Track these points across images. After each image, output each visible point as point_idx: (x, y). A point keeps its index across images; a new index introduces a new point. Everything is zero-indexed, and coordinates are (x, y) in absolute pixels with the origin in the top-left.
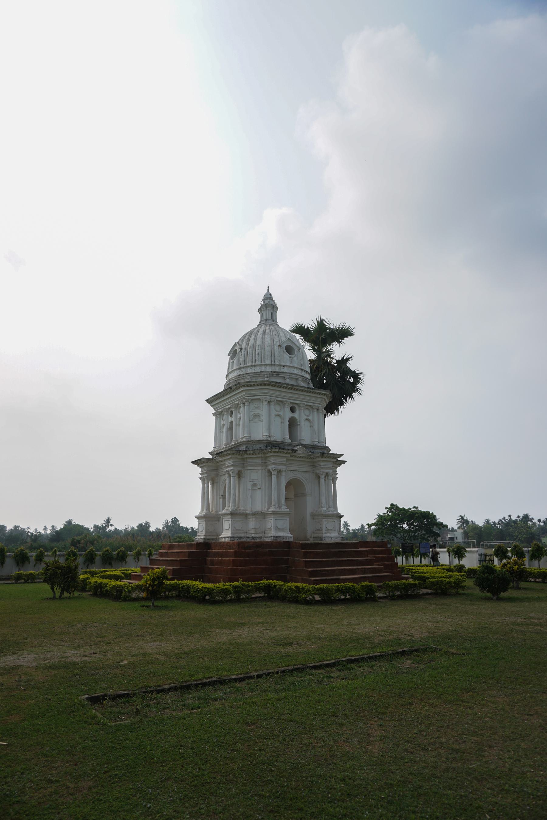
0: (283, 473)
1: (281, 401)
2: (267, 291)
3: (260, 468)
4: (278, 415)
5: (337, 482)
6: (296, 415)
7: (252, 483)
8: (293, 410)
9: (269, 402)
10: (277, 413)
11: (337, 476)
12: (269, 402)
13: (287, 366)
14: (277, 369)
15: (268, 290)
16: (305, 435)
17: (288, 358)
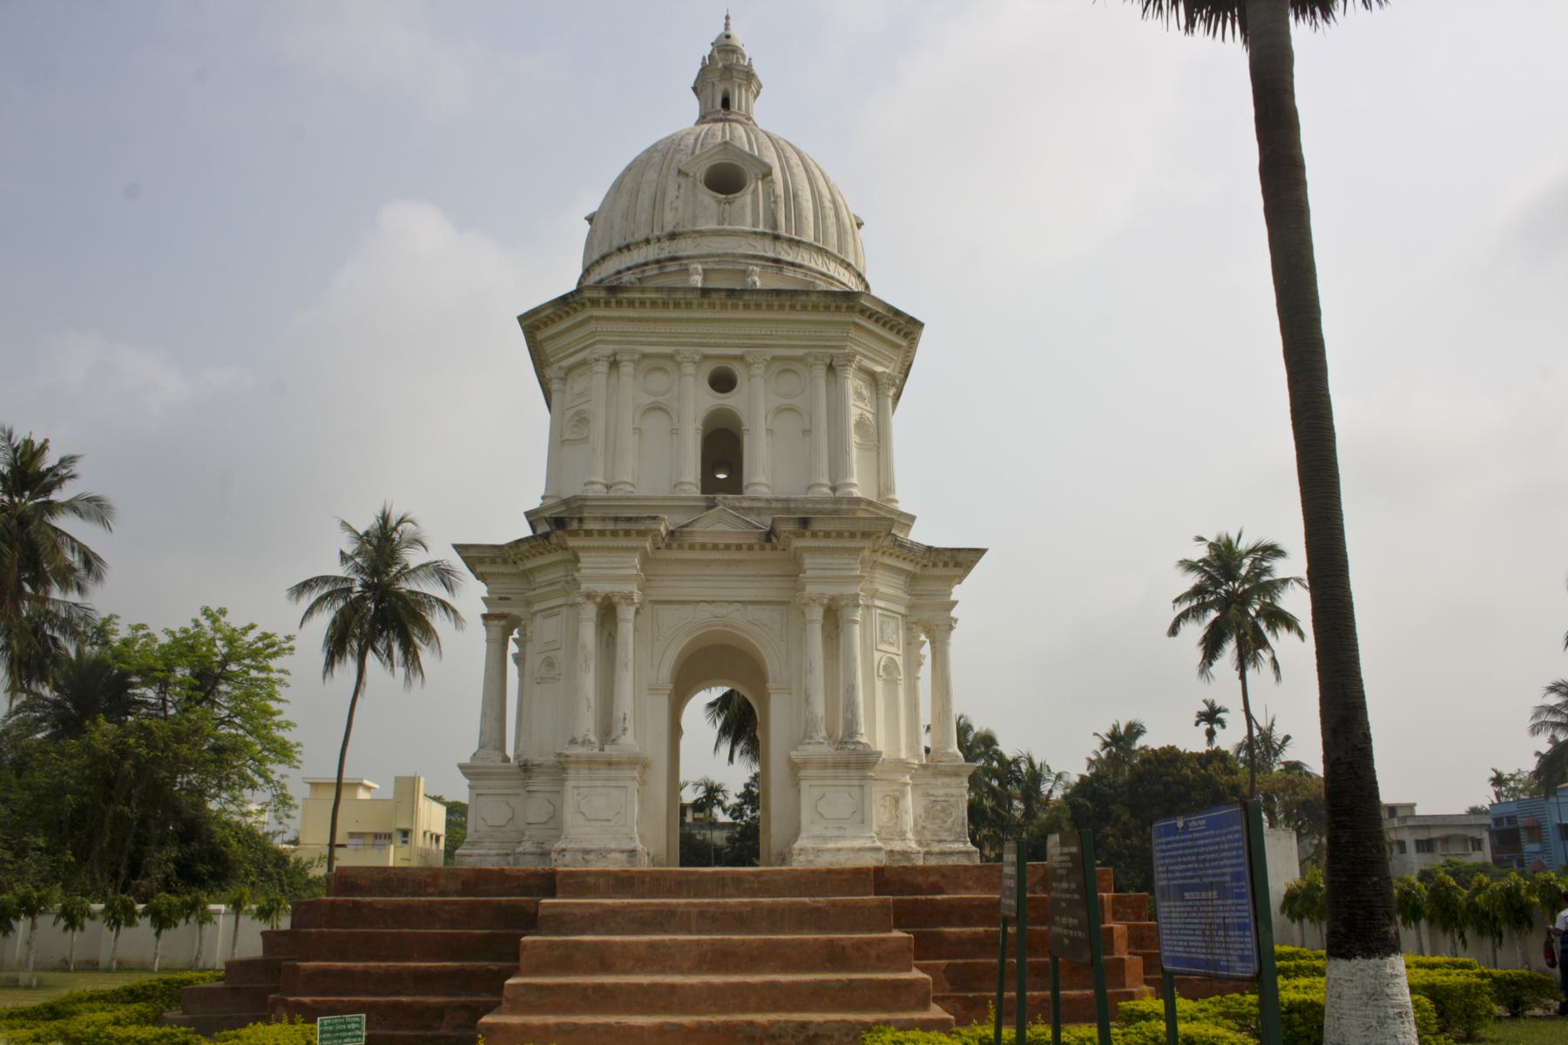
0: (627, 614)
1: (671, 357)
2: (722, 30)
3: (561, 601)
4: (656, 408)
5: (955, 637)
6: (730, 401)
7: (543, 656)
8: (723, 382)
9: (614, 364)
10: (652, 399)
11: (954, 613)
12: (614, 364)
13: (702, 233)
14: (667, 249)
15: (727, 26)
16: (768, 470)
17: (714, 204)
